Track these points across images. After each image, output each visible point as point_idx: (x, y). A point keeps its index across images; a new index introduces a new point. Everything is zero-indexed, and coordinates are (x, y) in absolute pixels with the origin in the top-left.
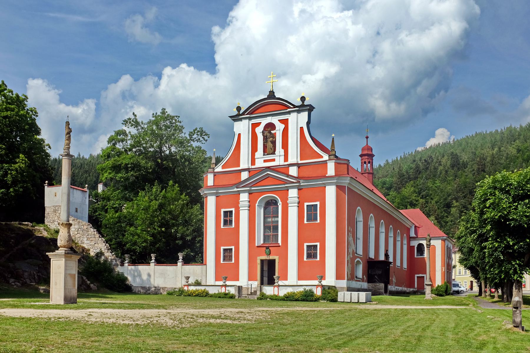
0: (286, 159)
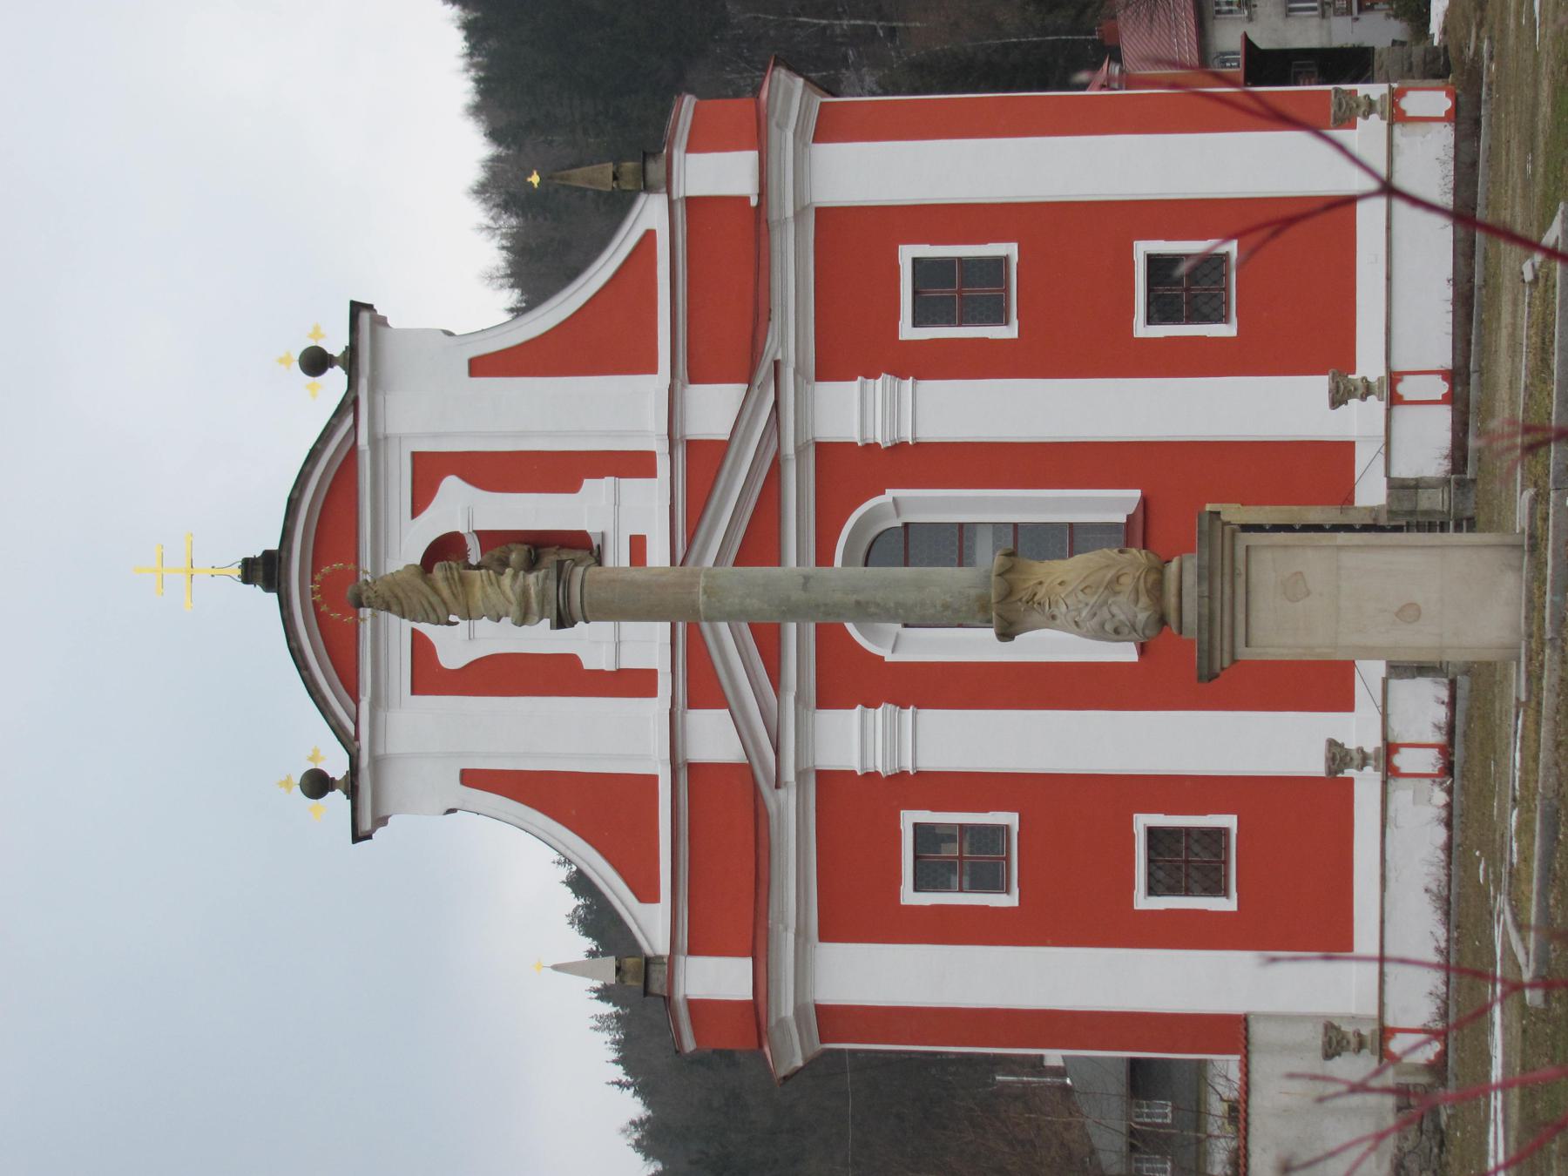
0: (637, 464)
